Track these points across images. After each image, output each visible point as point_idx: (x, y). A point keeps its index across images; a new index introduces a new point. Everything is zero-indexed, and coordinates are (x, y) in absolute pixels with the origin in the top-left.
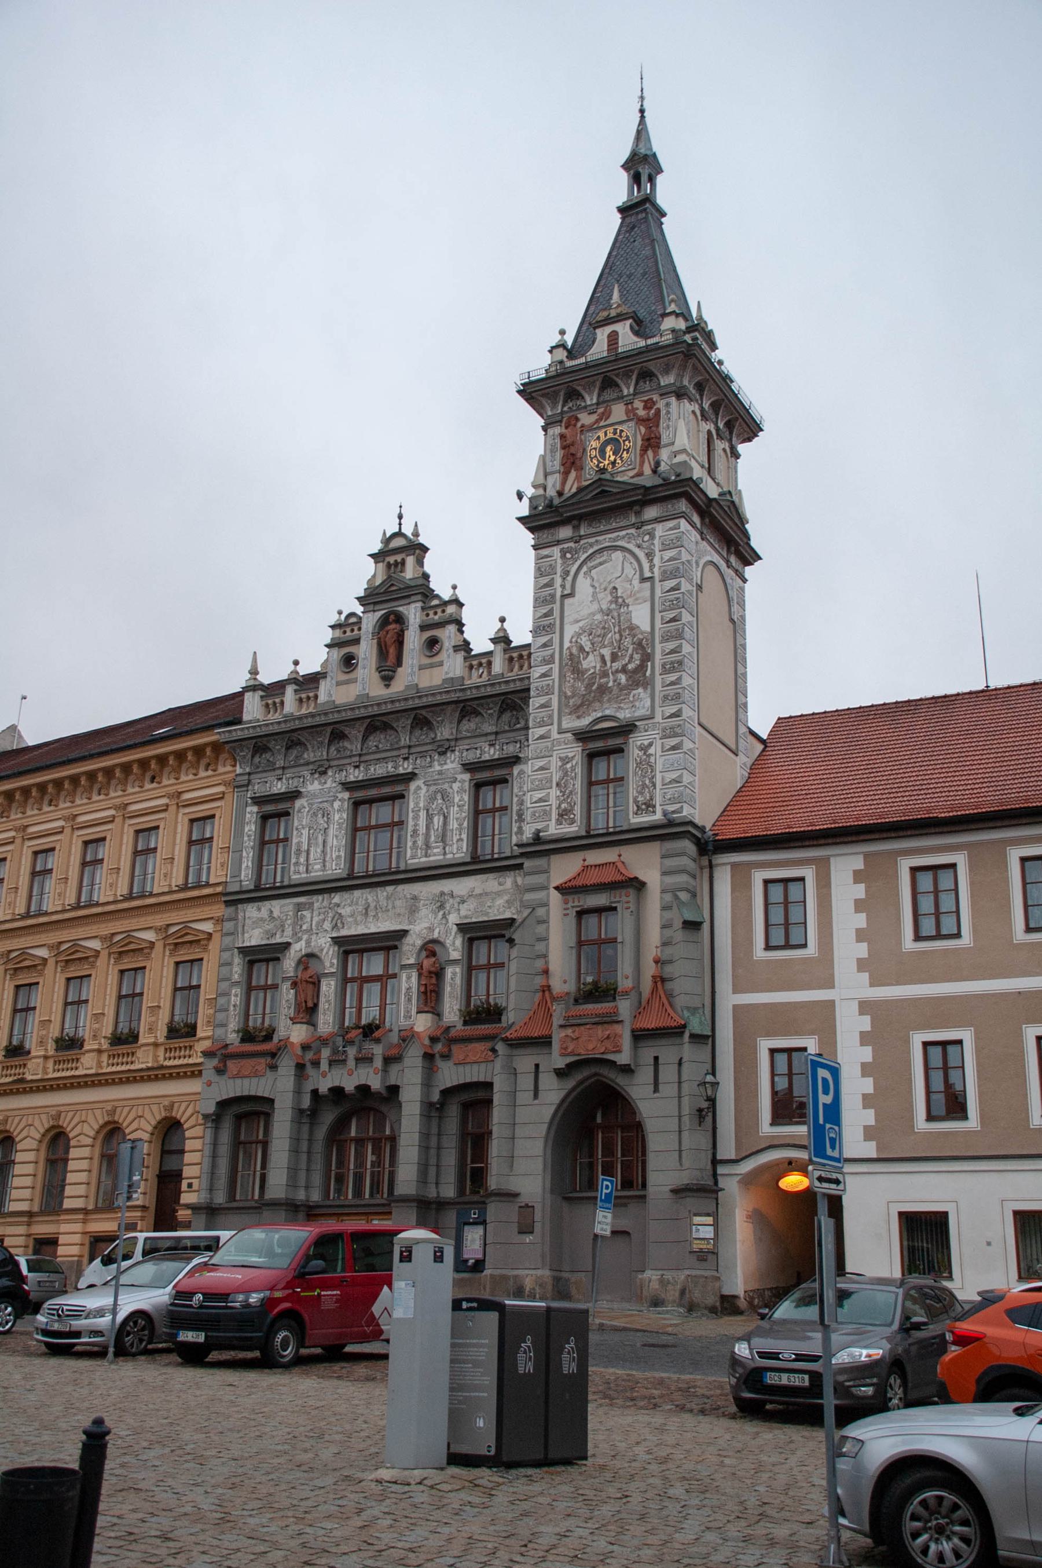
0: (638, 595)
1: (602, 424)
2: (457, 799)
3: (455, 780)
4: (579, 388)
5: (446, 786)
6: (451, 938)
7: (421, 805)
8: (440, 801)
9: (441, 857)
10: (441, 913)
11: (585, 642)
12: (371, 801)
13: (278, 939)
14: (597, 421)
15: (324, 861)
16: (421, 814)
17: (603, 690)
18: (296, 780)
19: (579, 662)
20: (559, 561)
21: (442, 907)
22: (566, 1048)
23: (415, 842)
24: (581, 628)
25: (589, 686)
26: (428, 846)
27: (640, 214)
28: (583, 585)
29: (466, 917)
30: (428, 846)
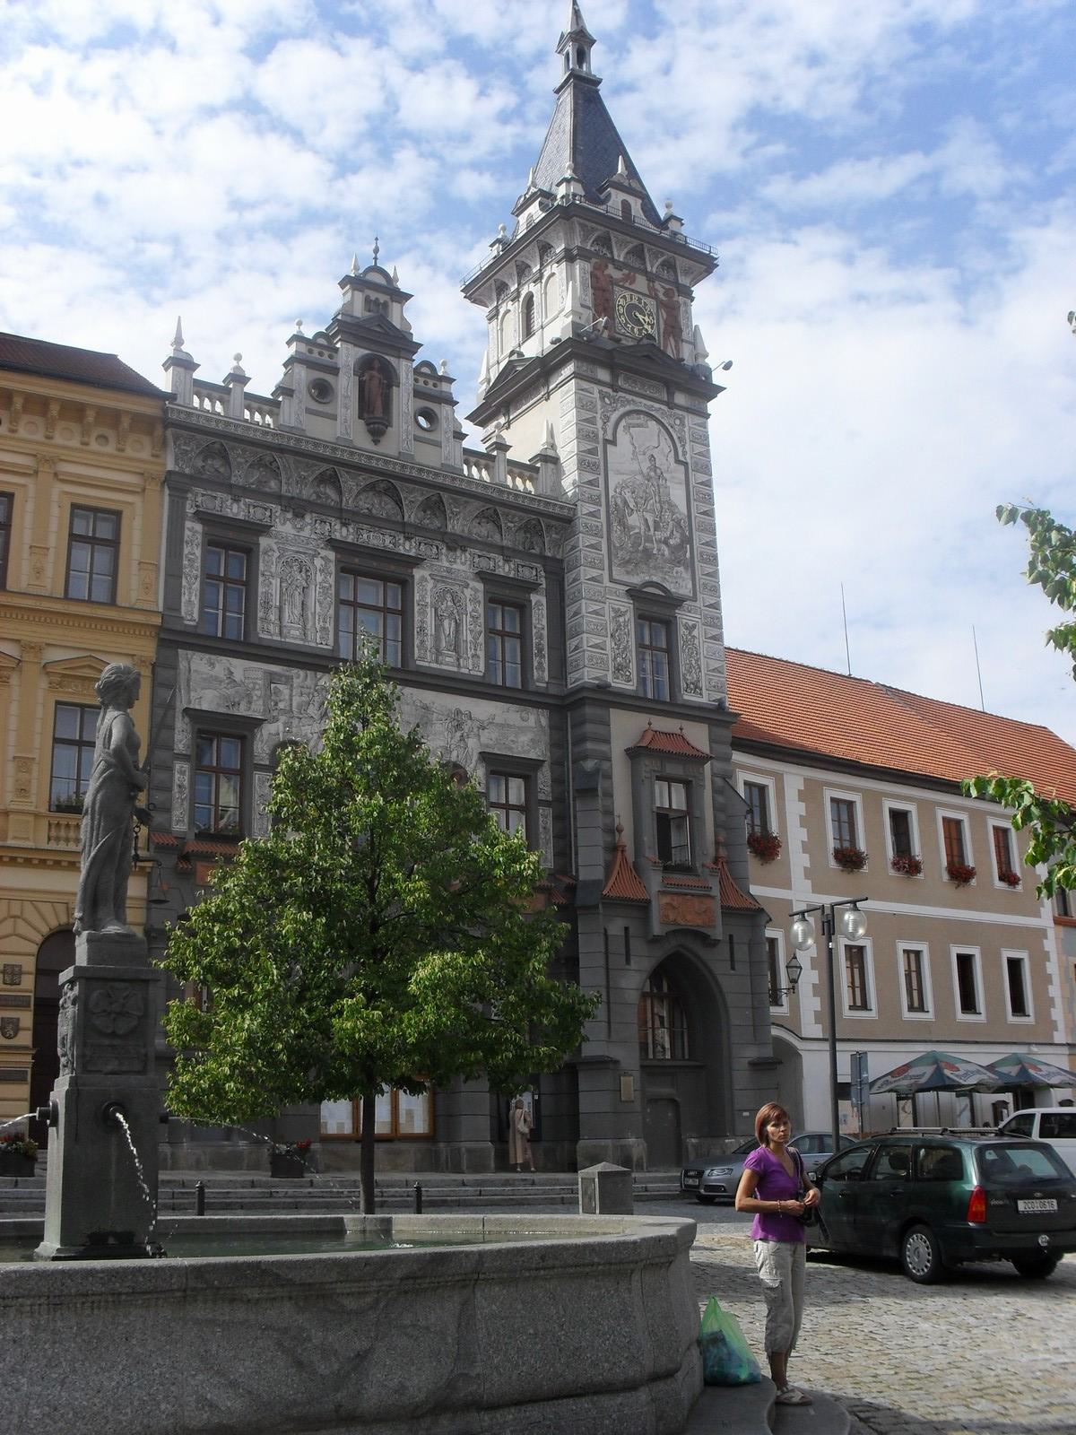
0: (674, 475)
1: (627, 285)
2: (470, 608)
3: (467, 586)
4: (613, 240)
5: (456, 588)
6: (472, 766)
7: (428, 600)
8: (449, 603)
9: (455, 669)
10: (458, 734)
11: (628, 496)
12: (356, 573)
13: (242, 711)
14: (622, 280)
15: (305, 627)
16: (428, 610)
17: (648, 554)
18: (260, 511)
19: (624, 516)
20: (599, 403)
21: (458, 727)
22: (667, 916)
23: (422, 642)
24: (624, 481)
25: (636, 544)
26: (438, 652)
27: (585, 90)
28: (622, 437)
29: (487, 746)
30: (438, 652)
